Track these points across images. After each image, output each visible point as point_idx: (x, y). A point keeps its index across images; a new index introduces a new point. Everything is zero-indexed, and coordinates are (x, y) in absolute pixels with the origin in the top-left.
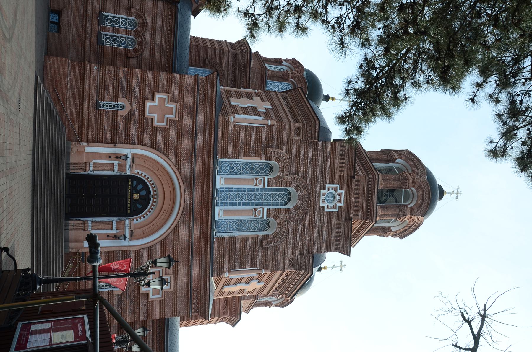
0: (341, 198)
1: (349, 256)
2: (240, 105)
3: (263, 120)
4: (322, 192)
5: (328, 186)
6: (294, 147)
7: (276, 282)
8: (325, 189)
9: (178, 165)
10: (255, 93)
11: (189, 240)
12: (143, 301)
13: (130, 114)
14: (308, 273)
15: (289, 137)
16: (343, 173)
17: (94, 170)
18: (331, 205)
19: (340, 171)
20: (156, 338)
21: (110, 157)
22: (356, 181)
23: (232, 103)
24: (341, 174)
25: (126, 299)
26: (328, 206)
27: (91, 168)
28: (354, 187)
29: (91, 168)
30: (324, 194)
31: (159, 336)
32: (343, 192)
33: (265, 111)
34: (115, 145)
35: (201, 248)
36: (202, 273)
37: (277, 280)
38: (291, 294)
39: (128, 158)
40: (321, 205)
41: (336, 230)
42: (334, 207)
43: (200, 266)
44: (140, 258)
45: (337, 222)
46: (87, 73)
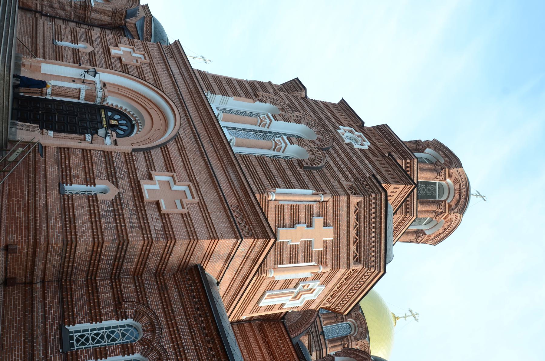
7: (348, 228)
11: (200, 148)
12: (152, 214)
17: (52, 94)
20: (196, 320)
21: (74, 81)
25: (122, 208)
27: (49, 91)
29: (49, 91)
31: (200, 315)
34: (80, 65)
35: (220, 160)
36: (236, 185)
37: (348, 223)
38: (380, 258)
39: (97, 73)
43: (229, 178)
44: (134, 162)
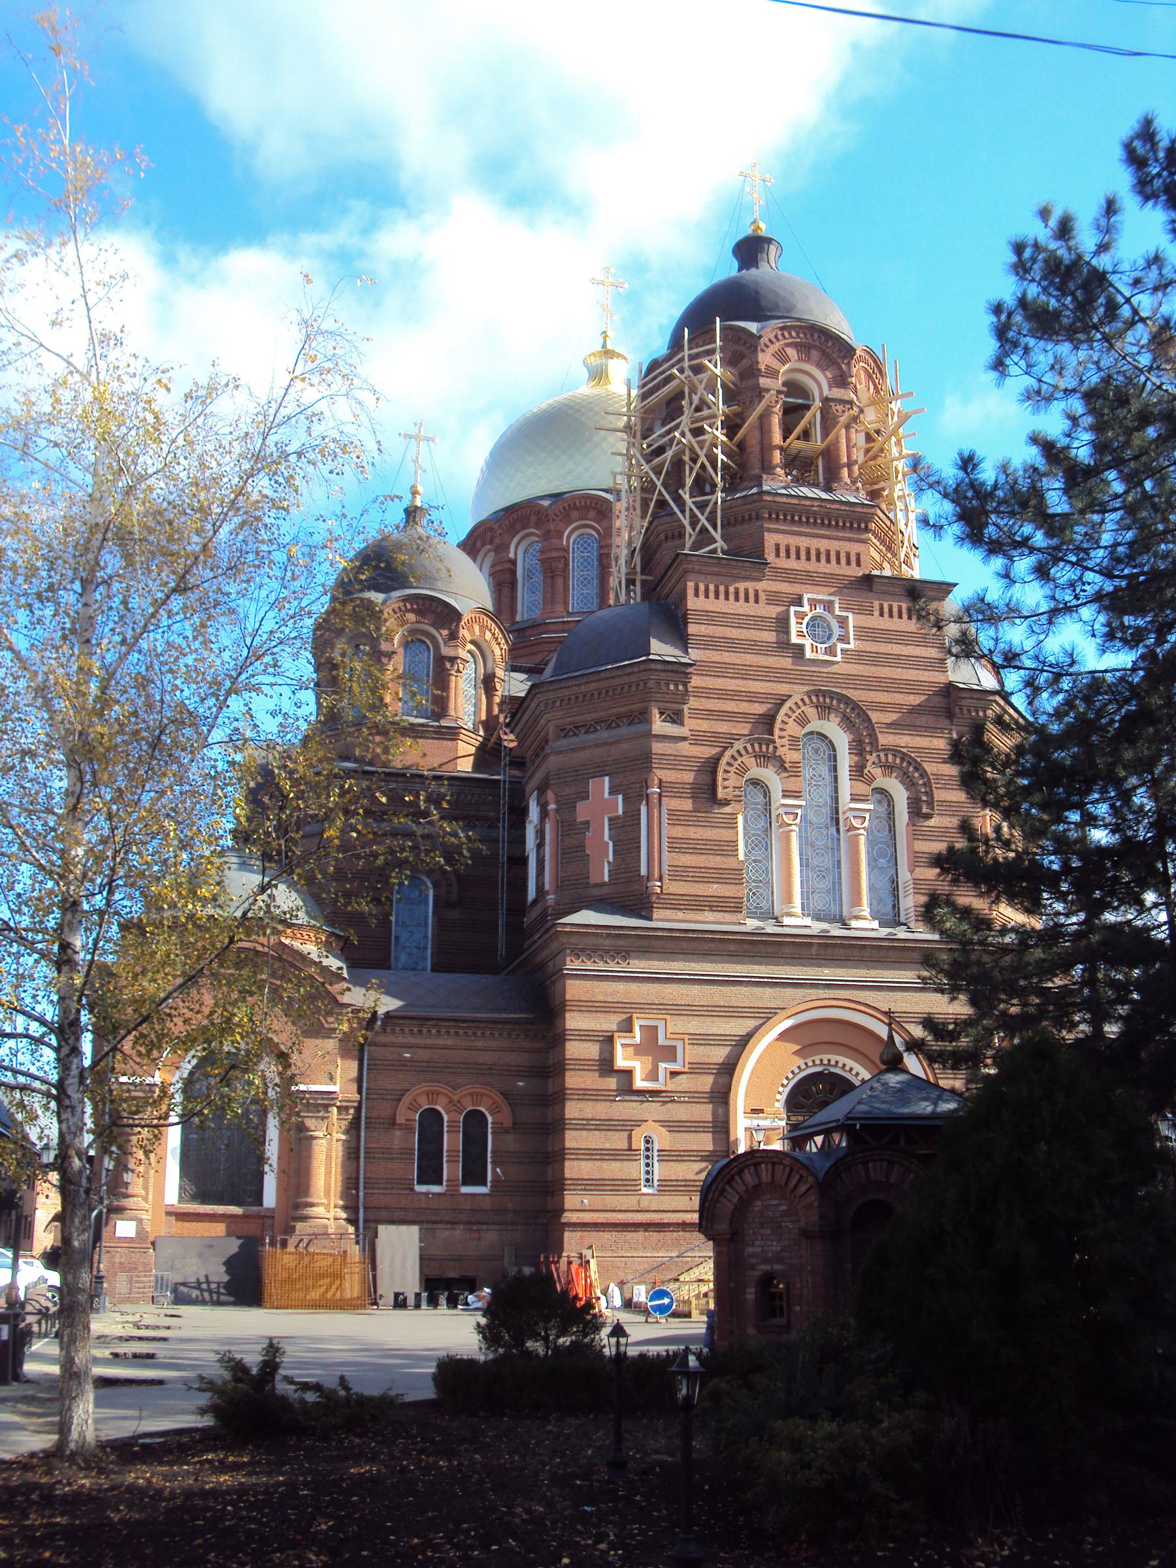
0: (820, 601)
1: (955, 585)
2: (611, 858)
3: (647, 804)
4: (808, 654)
5: (794, 639)
6: (705, 725)
8: (801, 648)
9: (767, 1016)
10: (557, 811)
13: (664, 1123)
14: (995, 701)
15: (684, 739)
16: (761, 594)
18: (837, 631)
19: (757, 601)
22: (778, 555)
23: (606, 879)
24: (762, 597)
26: (844, 639)
28: (792, 564)
30: (814, 649)
32: (806, 597)
33: (620, 797)
40: (839, 658)
41: (896, 619)
42: (843, 622)
45: (877, 613)
46: (587, 1217)
